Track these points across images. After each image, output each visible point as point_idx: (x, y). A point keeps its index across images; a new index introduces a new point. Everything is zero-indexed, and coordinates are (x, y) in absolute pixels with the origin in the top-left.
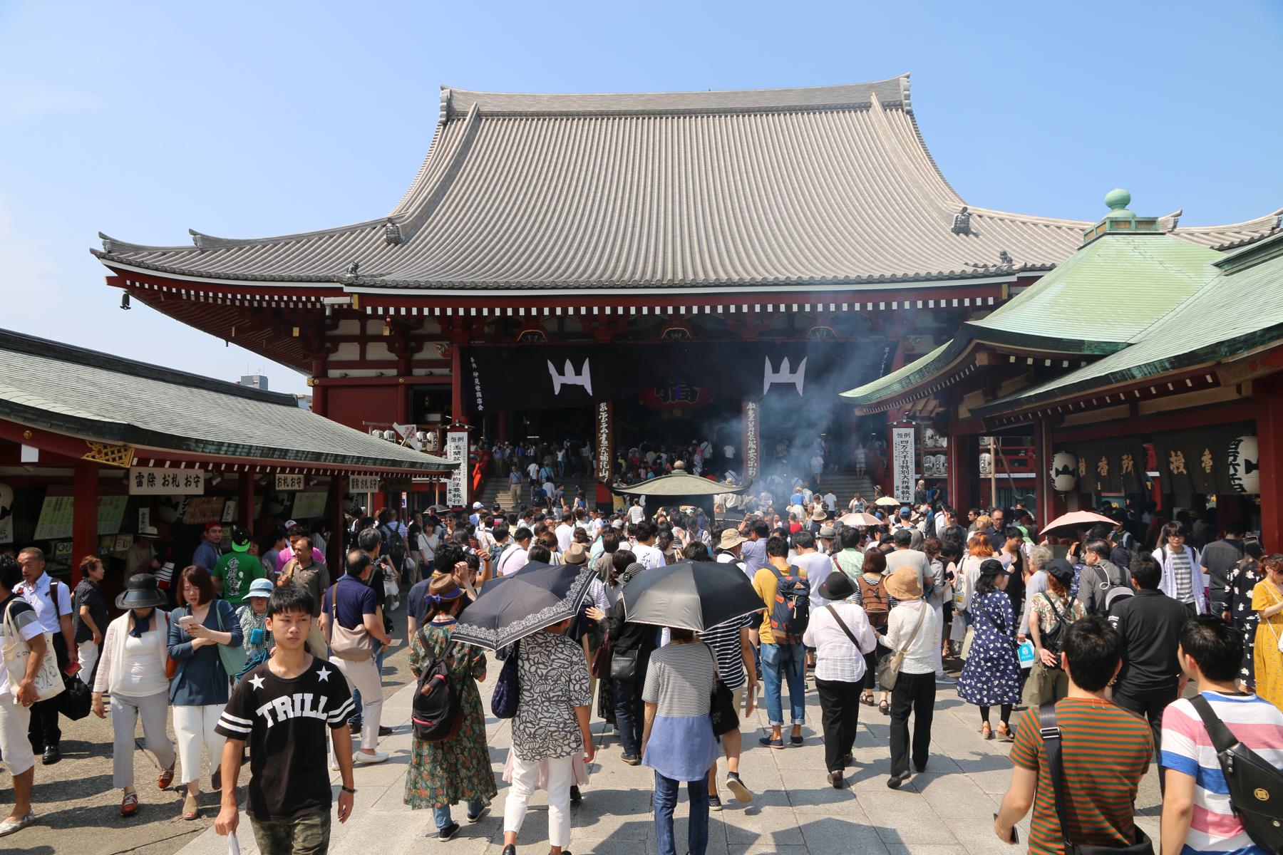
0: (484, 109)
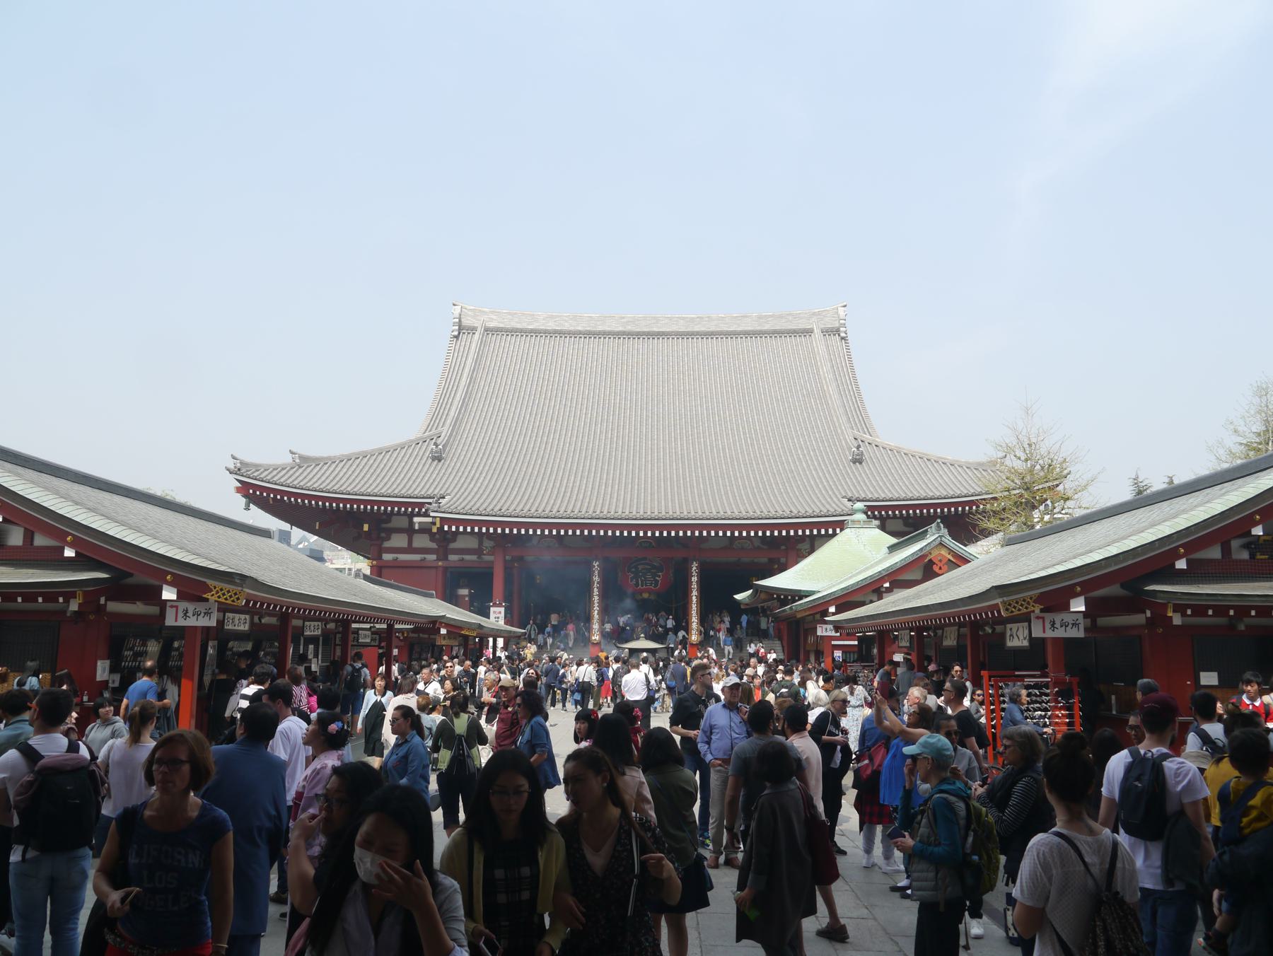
0: (492, 325)
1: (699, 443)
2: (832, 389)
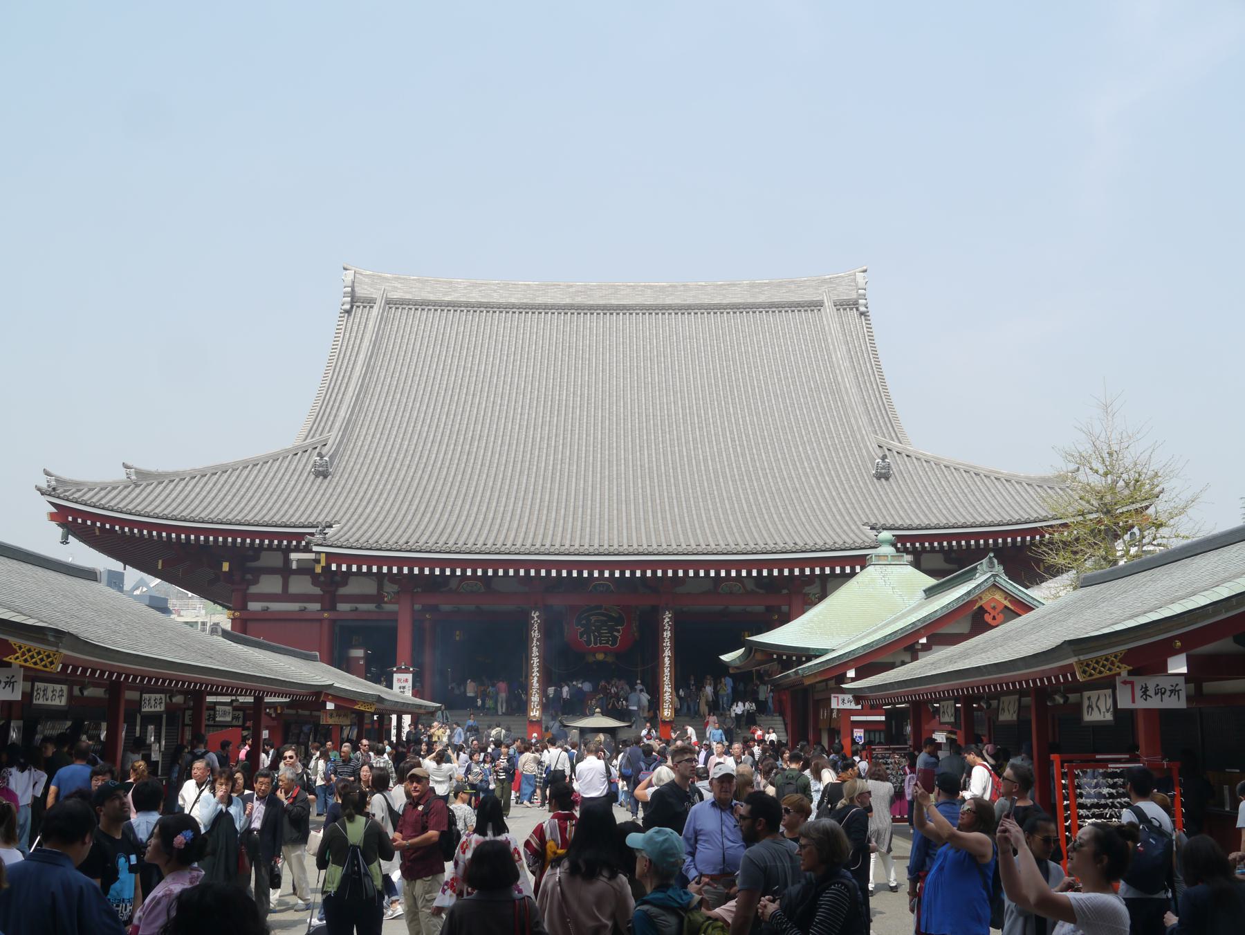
0: (395, 295)
1: (673, 453)
2: (848, 381)
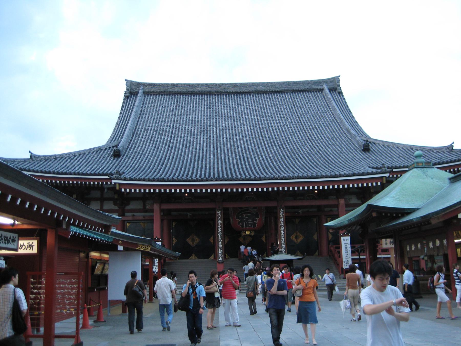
0: (147, 90)
